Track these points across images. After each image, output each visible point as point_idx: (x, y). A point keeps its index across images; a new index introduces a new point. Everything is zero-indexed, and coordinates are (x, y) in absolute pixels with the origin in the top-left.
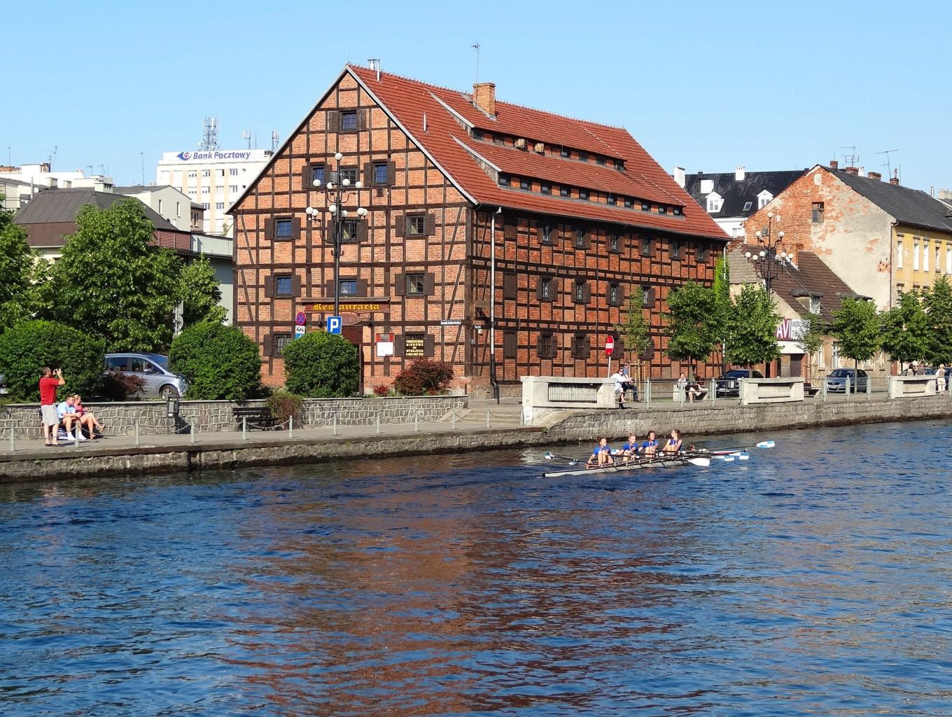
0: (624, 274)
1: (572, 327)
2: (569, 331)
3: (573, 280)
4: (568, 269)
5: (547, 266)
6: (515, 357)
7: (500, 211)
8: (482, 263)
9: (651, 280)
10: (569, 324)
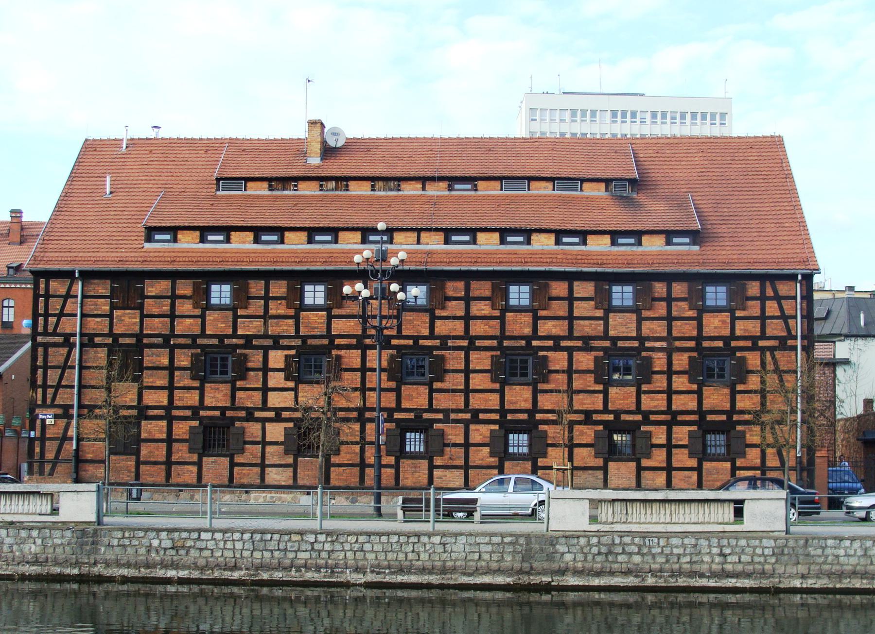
0: (444, 338)
1: (285, 414)
2: (278, 419)
3: (293, 352)
4: (276, 339)
5: (221, 338)
6: (137, 453)
7: (77, 275)
8: (60, 339)
9: (535, 343)
10: (278, 411)
